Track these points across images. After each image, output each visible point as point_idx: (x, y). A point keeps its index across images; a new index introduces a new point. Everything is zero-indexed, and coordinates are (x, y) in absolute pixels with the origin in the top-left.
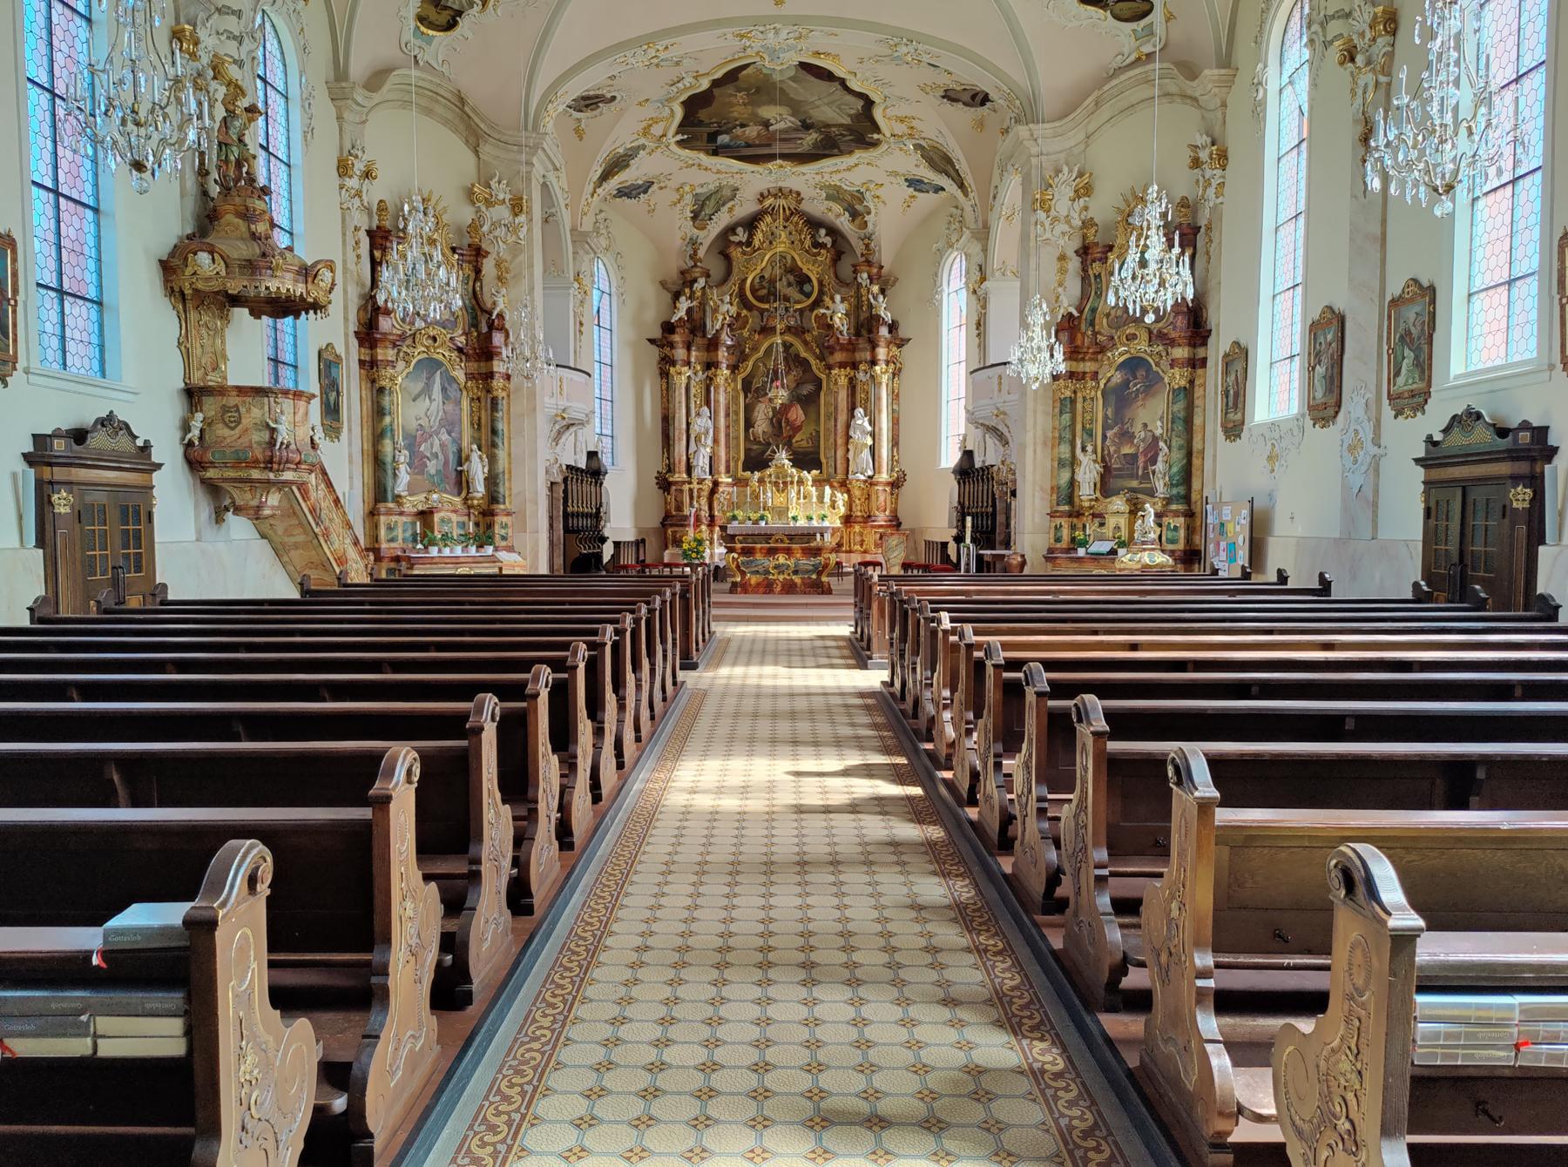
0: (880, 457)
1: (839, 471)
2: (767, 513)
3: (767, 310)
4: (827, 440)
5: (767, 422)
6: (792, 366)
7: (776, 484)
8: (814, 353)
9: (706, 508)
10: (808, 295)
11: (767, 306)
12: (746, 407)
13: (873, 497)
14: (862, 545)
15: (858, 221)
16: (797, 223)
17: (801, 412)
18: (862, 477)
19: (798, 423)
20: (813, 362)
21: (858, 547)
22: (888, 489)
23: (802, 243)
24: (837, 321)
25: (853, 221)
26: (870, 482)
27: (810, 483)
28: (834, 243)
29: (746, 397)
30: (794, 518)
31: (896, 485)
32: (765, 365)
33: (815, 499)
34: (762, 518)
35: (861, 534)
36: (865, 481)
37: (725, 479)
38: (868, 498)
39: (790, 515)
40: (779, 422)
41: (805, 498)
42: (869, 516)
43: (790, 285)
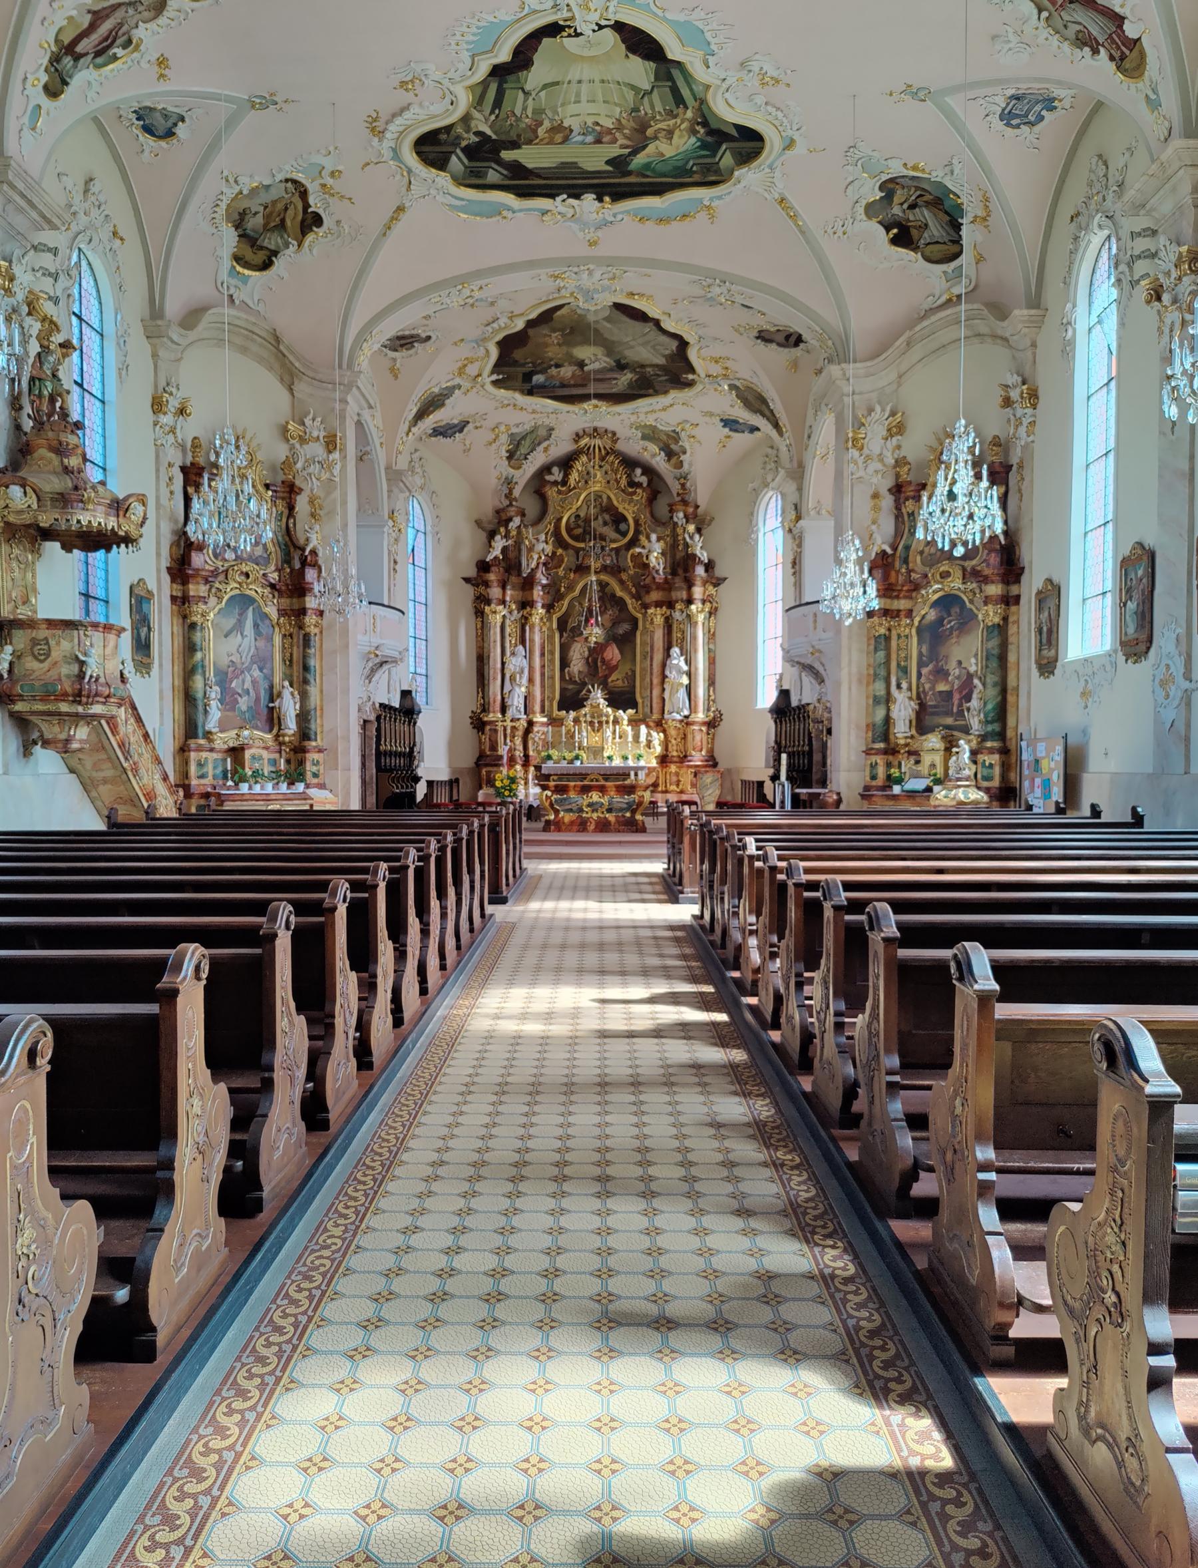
0: (696, 696)
1: (655, 711)
2: (582, 753)
3: (583, 549)
4: (642, 679)
6: (609, 606)
7: (591, 723)
8: (630, 593)
9: (521, 748)
13: (690, 737)
14: (678, 785)
16: (613, 463)
17: (616, 651)
19: (614, 662)
22: (704, 729)
23: (618, 482)
26: (687, 722)
27: (625, 722)
29: (561, 636)
30: (610, 758)
31: (712, 724)
33: (630, 739)
34: (577, 758)
35: (677, 774)
36: (681, 721)
37: (540, 719)
38: (685, 737)
39: (606, 754)
41: (620, 737)
43: (605, 524)
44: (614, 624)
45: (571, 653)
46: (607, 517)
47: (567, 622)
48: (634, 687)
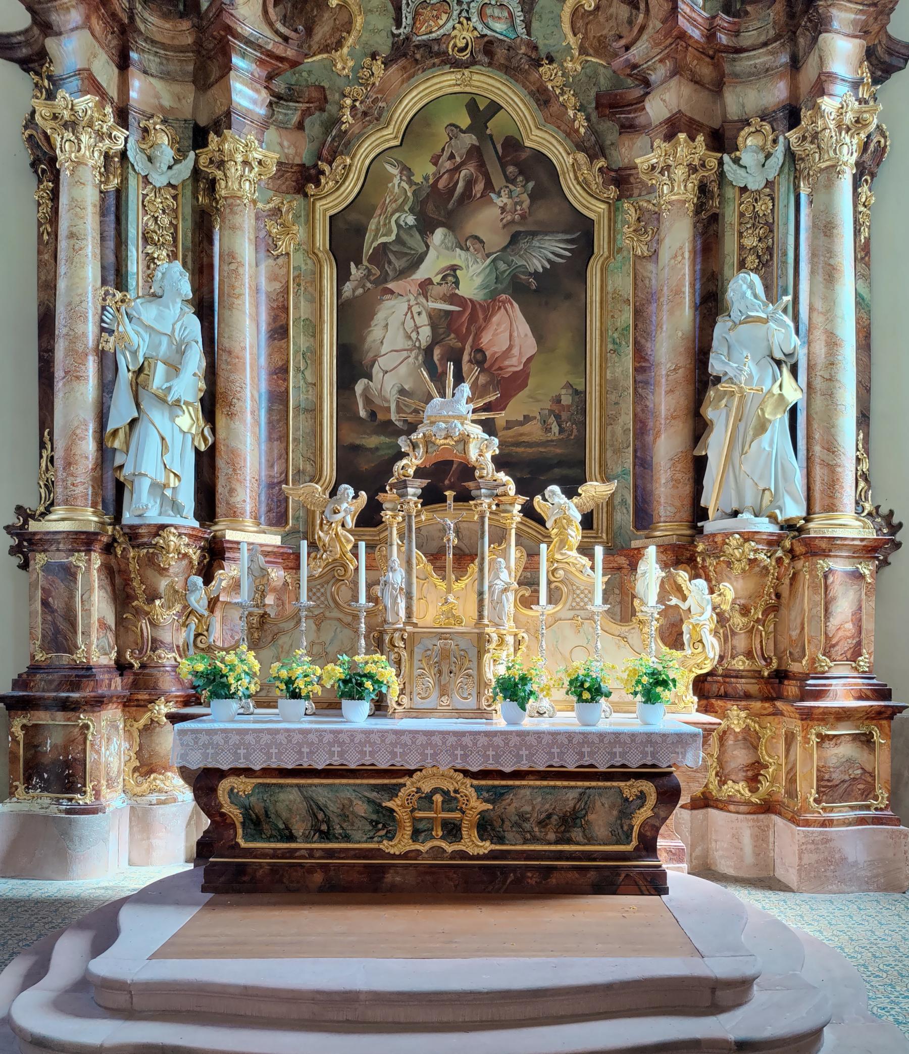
4: (607, 420)
5: (415, 359)
6: (498, 181)
8: (570, 133)
12: (344, 309)
14: (753, 781)
17: (523, 328)
18: (765, 526)
19: (514, 364)
21: (738, 788)
29: (343, 277)
32: (407, 171)
36: (773, 543)
41: (553, 598)
42: (781, 675)
44: (515, 239)
45: (375, 333)
47: (360, 231)
48: (581, 442)
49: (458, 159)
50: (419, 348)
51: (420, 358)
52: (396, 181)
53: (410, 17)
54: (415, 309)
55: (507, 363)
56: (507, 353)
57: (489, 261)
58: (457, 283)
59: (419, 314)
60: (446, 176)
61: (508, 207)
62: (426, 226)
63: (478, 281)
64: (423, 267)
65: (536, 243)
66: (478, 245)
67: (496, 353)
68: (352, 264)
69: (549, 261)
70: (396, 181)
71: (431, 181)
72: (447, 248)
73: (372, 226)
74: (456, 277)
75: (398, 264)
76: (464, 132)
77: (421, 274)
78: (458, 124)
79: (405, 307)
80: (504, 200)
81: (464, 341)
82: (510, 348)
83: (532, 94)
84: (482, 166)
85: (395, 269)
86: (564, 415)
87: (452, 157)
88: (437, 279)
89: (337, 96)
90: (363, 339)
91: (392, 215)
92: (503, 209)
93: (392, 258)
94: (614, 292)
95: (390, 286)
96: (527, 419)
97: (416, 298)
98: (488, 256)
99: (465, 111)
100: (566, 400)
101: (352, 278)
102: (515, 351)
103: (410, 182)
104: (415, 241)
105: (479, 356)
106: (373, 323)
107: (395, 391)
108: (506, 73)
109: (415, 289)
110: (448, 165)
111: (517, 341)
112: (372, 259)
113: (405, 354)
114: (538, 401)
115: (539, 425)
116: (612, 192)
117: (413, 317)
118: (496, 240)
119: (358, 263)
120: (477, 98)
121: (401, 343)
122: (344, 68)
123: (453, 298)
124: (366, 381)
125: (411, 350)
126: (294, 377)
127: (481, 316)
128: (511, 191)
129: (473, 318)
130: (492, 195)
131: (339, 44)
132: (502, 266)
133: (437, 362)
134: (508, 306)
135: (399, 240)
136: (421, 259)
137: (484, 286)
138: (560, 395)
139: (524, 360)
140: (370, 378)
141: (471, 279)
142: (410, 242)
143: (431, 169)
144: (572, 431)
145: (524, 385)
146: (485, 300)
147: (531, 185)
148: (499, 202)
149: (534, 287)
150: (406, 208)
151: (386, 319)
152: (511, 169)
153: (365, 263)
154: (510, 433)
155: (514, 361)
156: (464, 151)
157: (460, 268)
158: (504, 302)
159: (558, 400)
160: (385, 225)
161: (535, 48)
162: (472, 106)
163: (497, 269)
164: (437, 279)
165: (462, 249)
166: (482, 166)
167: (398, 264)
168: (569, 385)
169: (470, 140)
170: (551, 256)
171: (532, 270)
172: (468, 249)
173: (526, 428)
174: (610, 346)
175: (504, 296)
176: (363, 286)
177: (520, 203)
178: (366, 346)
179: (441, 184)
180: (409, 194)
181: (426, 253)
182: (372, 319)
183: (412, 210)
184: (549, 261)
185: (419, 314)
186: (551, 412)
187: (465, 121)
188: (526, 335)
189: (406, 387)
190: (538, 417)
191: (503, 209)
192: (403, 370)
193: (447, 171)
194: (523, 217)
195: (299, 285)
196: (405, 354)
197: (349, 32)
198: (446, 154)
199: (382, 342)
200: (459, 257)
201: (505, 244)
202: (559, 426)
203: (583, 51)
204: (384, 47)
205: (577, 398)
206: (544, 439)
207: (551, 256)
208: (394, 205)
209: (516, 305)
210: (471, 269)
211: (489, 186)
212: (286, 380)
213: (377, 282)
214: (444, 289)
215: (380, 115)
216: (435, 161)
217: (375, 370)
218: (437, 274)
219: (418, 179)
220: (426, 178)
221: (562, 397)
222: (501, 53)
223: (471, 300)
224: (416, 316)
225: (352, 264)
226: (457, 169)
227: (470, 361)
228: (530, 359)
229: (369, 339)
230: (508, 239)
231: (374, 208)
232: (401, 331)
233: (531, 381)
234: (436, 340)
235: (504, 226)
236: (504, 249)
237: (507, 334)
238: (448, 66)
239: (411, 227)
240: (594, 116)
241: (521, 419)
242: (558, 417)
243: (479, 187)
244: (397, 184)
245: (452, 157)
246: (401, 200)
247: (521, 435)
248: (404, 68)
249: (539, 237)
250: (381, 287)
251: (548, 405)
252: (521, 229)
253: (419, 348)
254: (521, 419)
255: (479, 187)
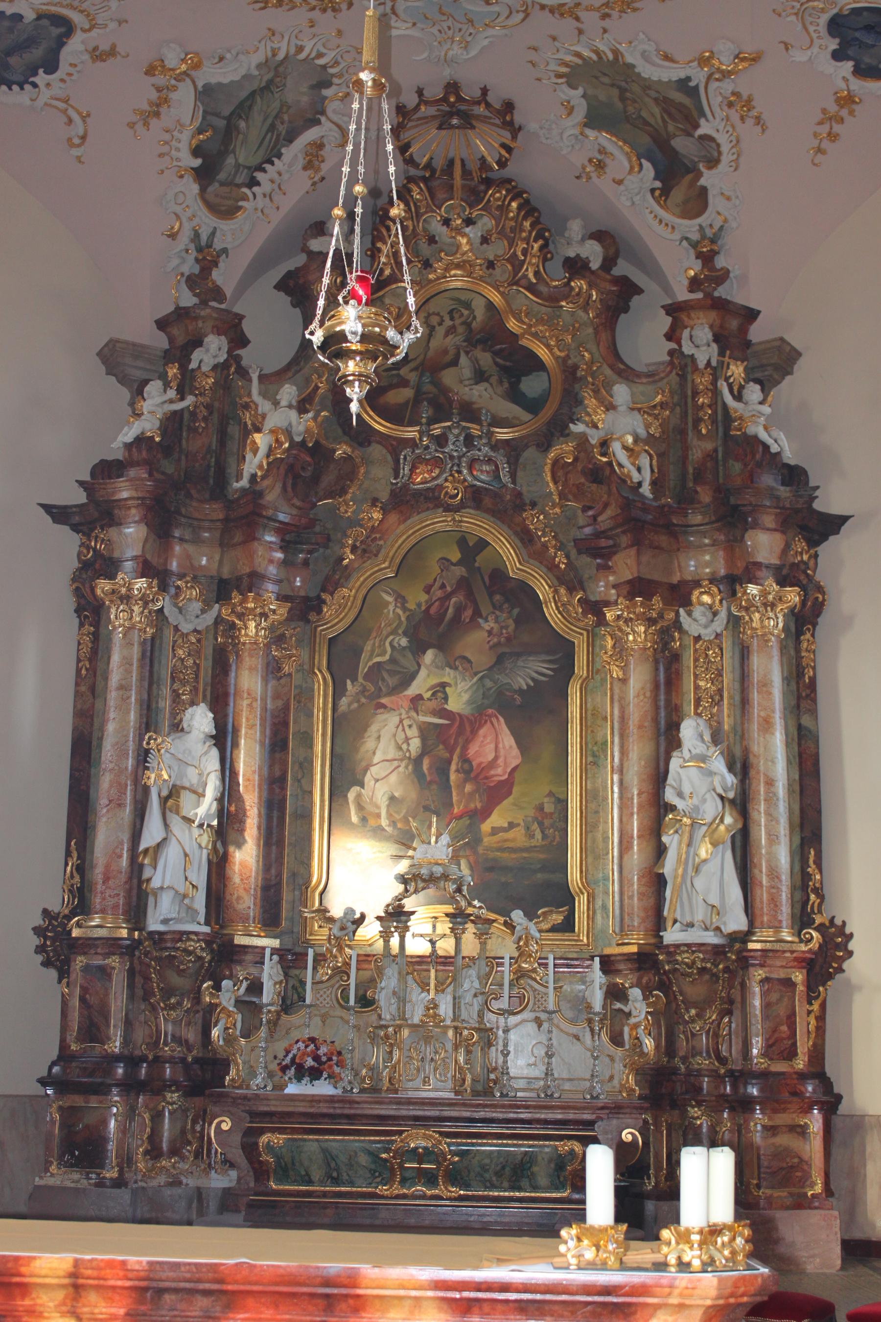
0: (758, 904)
3: (412, 443)
4: (589, 826)
6: (485, 608)
8: (552, 567)
10: (533, 406)
11: (411, 432)
15: (678, 194)
16: (504, 209)
17: (508, 740)
19: (500, 773)
20: (543, 589)
23: (517, 265)
24: (622, 456)
25: (666, 192)
28: (608, 263)
29: (339, 692)
32: (401, 599)
40: (442, 770)
43: (480, 376)
44: (500, 660)
46: (485, 359)
47: (357, 653)
49: (449, 589)
50: (409, 758)
51: (410, 767)
52: (391, 607)
53: (407, 468)
54: (406, 722)
55: (492, 772)
56: (493, 764)
57: (475, 679)
58: (446, 699)
59: (410, 726)
60: (437, 603)
61: (495, 631)
62: (418, 647)
63: (466, 697)
64: (415, 683)
65: (520, 663)
66: (468, 665)
67: (481, 763)
68: (349, 682)
69: (533, 679)
70: (391, 607)
71: (423, 608)
72: (437, 667)
73: (368, 647)
74: (445, 693)
75: (391, 681)
76: (455, 565)
77: (413, 690)
78: (449, 557)
79: (396, 720)
80: (490, 625)
81: (452, 753)
82: (496, 758)
83: (516, 534)
84: (470, 596)
85: (388, 685)
86: (547, 822)
87: (443, 586)
88: (427, 695)
89: (339, 535)
90: (356, 750)
91: (387, 637)
92: (490, 633)
93: (386, 675)
94: (594, 709)
95: (384, 701)
96: (512, 825)
97: (407, 712)
98: (476, 674)
99: (455, 547)
100: (549, 808)
101: (348, 693)
102: (500, 761)
103: (404, 609)
104: (408, 662)
105: (466, 766)
106: (367, 735)
107: (385, 798)
108: (493, 516)
109: (406, 704)
110: (439, 594)
111: (502, 753)
112: (366, 677)
113: (396, 763)
114: (522, 808)
115: (523, 831)
116: (591, 619)
117: (404, 730)
118: (482, 660)
119: (354, 680)
120: (467, 536)
121: (392, 753)
122: (346, 512)
123: (443, 713)
124: (358, 788)
125: (401, 760)
126: (292, 785)
127: (468, 729)
128: (497, 617)
129: (460, 732)
130: (480, 620)
131: (343, 491)
132: (488, 683)
133: (426, 771)
134: (494, 720)
135: (392, 660)
136: (413, 677)
137: (470, 702)
138: (543, 804)
139: (509, 770)
140: (362, 786)
141: (460, 695)
142: (403, 661)
143: (423, 597)
144: (554, 837)
145: (509, 793)
146: (473, 715)
147: (516, 611)
148: (486, 626)
149: (518, 703)
150: (400, 632)
151: (379, 731)
152: (497, 597)
153: (360, 679)
154: (495, 838)
155: (499, 771)
156: (454, 581)
157: (449, 685)
158: (490, 716)
159: (540, 808)
160: (380, 646)
161: (519, 495)
162: (462, 542)
163: (483, 686)
164: (427, 695)
165: (451, 668)
166: (470, 596)
167: (391, 681)
168: (551, 794)
169: (460, 571)
170: (535, 675)
171: (516, 687)
172: (456, 668)
173: (510, 835)
174: (590, 759)
175: (490, 711)
176: (358, 701)
177: (507, 627)
178: (359, 756)
179: (433, 610)
180: (403, 619)
181: (418, 672)
182: (365, 730)
183: (405, 634)
184: (533, 679)
185: (410, 726)
186: (535, 819)
187: (455, 555)
188: (511, 747)
189: (396, 794)
190: (522, 824)
191: (490, 633)
192: (393, 778)
193: (439, 599)
194: (509, 639)
195: (299, 702)
196: (396, 763)
197: (352, 481)
198: (438, 584)
199: (374, 753)
200: (448, 675)
201: (492, 663)
202: (543, 832)
203: (562, 495)
204: (384, 496)
205: (559, 807)
206: (527, 844)
207: (535, 675)
208: (389, 629)
209: (502, 719)
210: (459, 686)
211: (477, 613)
212: (283, 788)
213: (371, 698)
214: (433, 704)
215: (378, 552)
216: (428, 590)
217: (368, 779)
218: (428, 690)
219: (411, 605)
220: (419, 605)
221: (546, 805)
222: (487, 501)
223: (459, 714)
224: (407, 729)
225: (349, 682)
226: (448, 597)
227: (457, 771)
228: (514, 769)
229: (363, 750)
230: (494, 660)
231: (370, 631)
232: (393, 742)
233: (515, 789)
234: (425, 751)
235: (491, 648)
236: (490, 669)
237: (493, 746)
238: (441, 510)
239: (404, 648)
240: (573, 553)
241: (506, 825)
242: (541, 824)
243: (468, 613)
244: (392, 609)
245: (443, 586)
246: (395, 625)
247: (506, 840)
248: (401, 512)
249: (524, 658)
250: (374, 702)
251: (531, 812)
252: (507, 650)
253: (409, 758)
254: (506, 825)
255: (468, 613)
